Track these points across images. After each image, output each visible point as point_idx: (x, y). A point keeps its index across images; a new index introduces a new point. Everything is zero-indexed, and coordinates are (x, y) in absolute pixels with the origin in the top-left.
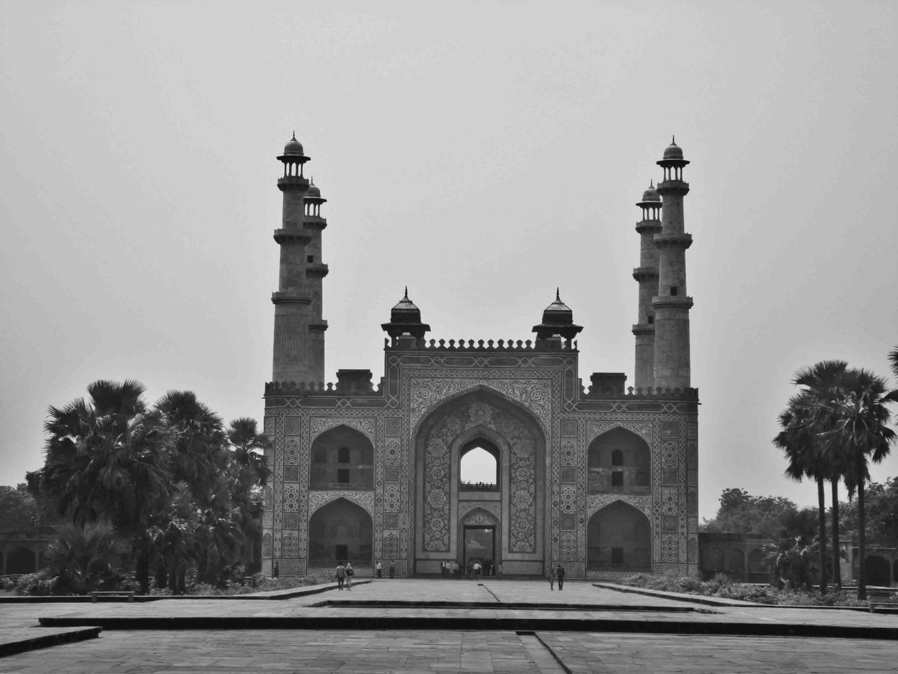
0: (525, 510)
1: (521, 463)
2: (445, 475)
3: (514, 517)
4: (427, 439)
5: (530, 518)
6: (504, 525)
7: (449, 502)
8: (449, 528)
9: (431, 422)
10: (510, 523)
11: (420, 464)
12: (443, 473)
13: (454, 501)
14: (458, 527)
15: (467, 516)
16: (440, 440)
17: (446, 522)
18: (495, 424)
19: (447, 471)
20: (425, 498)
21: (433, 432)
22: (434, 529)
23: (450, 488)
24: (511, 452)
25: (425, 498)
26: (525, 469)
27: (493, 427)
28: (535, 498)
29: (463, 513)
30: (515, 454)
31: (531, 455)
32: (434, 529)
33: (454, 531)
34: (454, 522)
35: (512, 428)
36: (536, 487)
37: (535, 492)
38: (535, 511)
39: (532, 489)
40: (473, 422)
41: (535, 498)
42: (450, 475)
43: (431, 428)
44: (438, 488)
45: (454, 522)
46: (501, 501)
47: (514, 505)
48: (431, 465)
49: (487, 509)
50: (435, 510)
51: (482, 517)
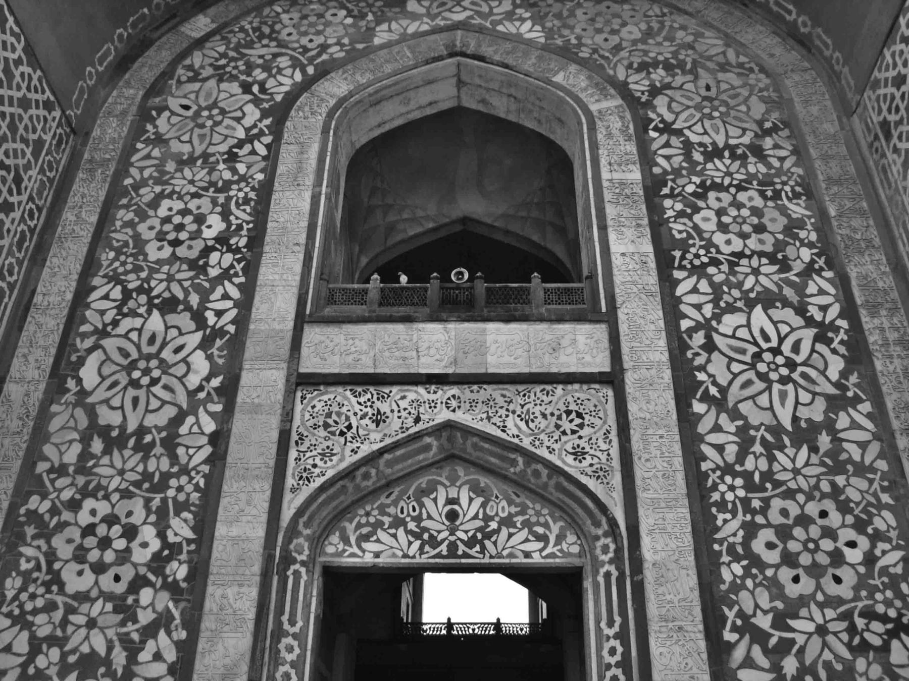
0: (804, 434)
1: (716, 170)
2: (222, 240)
3: (729, 490)
4: (157, 88)
5: (855, 489)
6: (651, 548)
7: (229, 391)
8: (199, 572)
9: (201, 24)
10: (703, 531)
11: (88, 192)
12: (215, 226)
13: (263, 381)
14: (274, 565)
15: (352, 494)
16: (235, 88)
17: (181, 529)
18: (538, 19)
19: (241, 215)
20: (64, 365)
21: (197, 59)
22: (77, 580)
23: (245, 305)
24: (643, 125)
25: (64, 365)
26: (751, 197)
27: (528, 30)
28: (858, 354)
29: (323, 461)
30: (667, 128)
31: (768, 133)
32: (77, 580)
33: (233, 598)
34: (241, 526)
35: (632, 32)
36: (843, 282)
37: (850, 311)
38: (884, 434)
39: (822, 293)
40: (414, 17)
41: (858, 354)
42: (257, 240)
43: (199, 43)
44: (169, 306)
45: (241, 526)
46: (613, 379)
47: (719, 403)
48: (147, 194)
49: (514, 429)
50: (115, 441)
51: (470, 508)
